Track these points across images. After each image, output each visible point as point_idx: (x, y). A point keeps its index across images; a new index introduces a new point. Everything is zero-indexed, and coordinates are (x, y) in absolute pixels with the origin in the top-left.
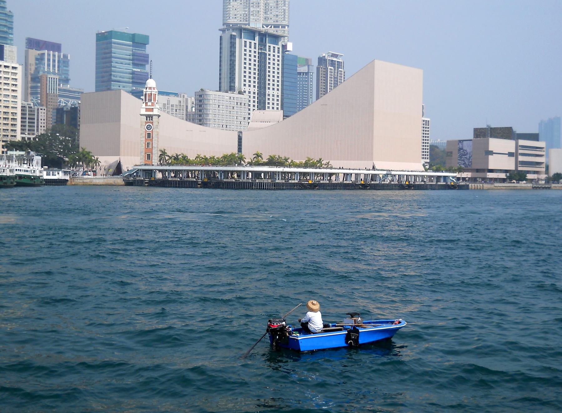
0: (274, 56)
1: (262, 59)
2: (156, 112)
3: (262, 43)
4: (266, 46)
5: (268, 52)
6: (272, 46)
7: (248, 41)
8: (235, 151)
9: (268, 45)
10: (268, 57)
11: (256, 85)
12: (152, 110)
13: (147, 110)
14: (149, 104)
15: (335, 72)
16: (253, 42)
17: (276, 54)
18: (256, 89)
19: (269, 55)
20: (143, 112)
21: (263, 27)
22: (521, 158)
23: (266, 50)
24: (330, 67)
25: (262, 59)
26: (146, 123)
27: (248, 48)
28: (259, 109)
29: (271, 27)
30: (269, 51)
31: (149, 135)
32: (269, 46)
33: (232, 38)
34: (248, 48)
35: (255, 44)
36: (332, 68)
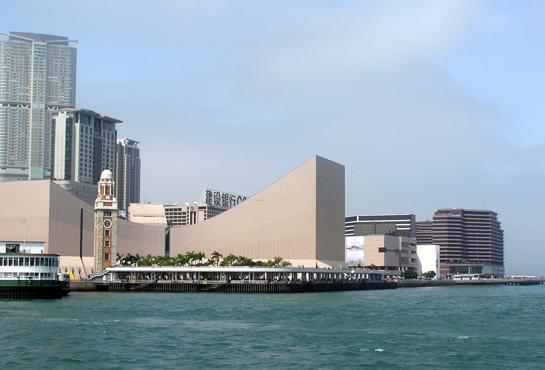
0: (108, 142)
4: (100, 131)
6: (107, 132)
7: (85, 126)
9: (103, 131)
10: (103, 144)
11: (92, 174)
12: (110, 204)
15: (131, 160)
16: (89, 127)
17: (110, 141)
19: (104, 141)
20: (100, 206)
21: (46, 108)
23: (100, 136)
26: (104, 218)
29: (56, 109)
30: (104, 137)
31: (107, 232)
32: (104, 132)
35: (91, 129)
36: (129, 156)
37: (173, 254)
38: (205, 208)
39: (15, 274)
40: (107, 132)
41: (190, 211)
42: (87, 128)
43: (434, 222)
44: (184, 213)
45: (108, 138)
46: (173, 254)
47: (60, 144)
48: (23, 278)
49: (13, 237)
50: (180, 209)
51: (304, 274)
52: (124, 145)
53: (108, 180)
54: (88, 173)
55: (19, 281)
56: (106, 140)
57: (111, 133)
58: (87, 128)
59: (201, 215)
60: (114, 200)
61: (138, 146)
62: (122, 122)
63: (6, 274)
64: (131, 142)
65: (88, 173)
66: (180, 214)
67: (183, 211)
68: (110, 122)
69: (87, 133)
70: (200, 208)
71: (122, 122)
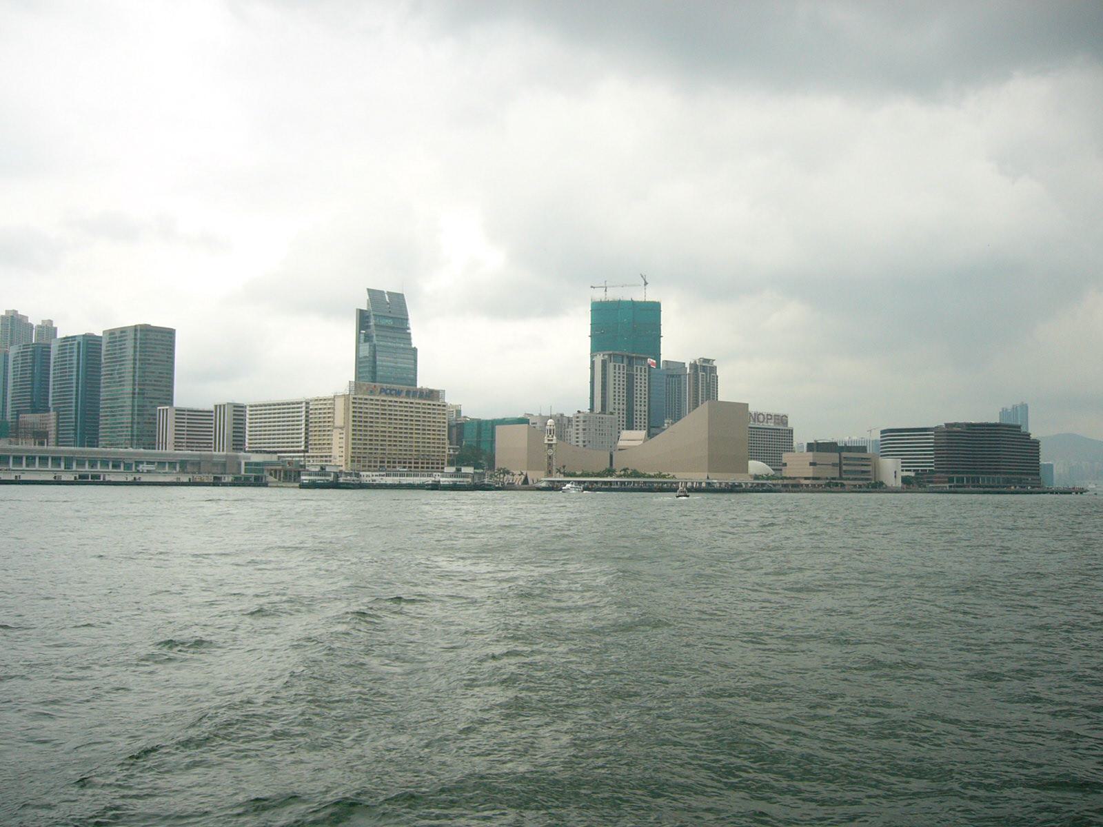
1: (630, 379)
2: (554, 442)
3: (630, 364)
5: (635, 373)
8: (608, 466)
13: (549, 440)
16: (622, 365)
20: (546, 442)
22: (844, 468)
25: (630, 379)
27: (617, 371)
28: (628, 429)
34: (617, 371)
51: (693, 483)
60: (555, 437)
61: (715, 363)
69: (619, 369)
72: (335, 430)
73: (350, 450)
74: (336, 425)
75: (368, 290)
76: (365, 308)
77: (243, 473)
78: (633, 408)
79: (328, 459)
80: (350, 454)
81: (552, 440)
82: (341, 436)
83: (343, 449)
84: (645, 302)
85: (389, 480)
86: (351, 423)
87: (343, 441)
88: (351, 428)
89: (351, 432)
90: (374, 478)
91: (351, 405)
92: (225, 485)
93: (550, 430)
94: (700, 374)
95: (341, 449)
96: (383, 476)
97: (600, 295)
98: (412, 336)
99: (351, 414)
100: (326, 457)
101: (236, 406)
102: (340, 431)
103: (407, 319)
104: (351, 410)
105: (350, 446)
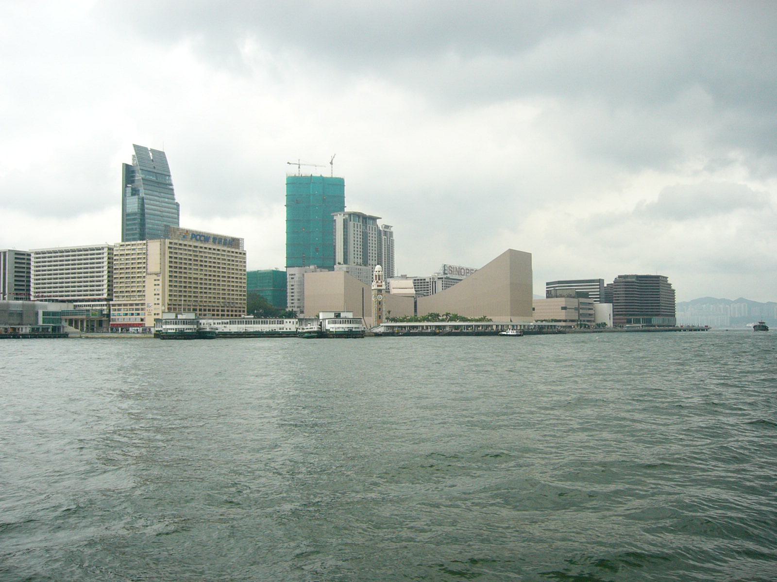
1: (365, 236)
11: (361, 257)
13: (378, 286)
14: (380, 282)
16: (359, 224)
17: (374, 232)
18: (361, 260)
22: (581, 311)
24: (383, 237)
25: (365, 236)
33: (345, 221)
34: (356, 229)
37: (419, 315)
38: (442, 278)
39: (343, 328)
40: (371, 226)
41: (431, 280)
42: (357, 225)
43: (615, 285)
44: (428, 282)
45: (372, 231)
46: (419, 315)
47: (339, 237)
48: (347, 330)
49: (338, 310)
50: (425, 280)
52: (381, 229)
53: (379, 271)
54: (359, 256)
55: (345, 331)
56: (371, 232)
57: (374, 227)
58: (357, 225)
59: (439, 284)
61: (392, 229)
62: (381, 218)
63: (338, 328)
64: (387, 227)
65: (359, 256)
66: (424, 283)
67: (426, 281)
68: (374, 219)
70: (439, 278)
71: (381, 218)
72: (148, 277)
73: (167, 298)
74: (149, 271)
75: (135, 146)
76: (130, 163)
77: (40, 323)
78: (367, 261)
79: (140, 307)
80: (167, 301)
81: (381, 286)
82: (157, 282)
83: (160, 297)
84: (332, 178)
85: (234, 328)
86: (167, 269)
87: (160, 287)
88: (167, 274)
89: (167, 279)
90: (216, 326)
91: (167, 251)
92: (25, 336)
93: (379, 276)
94: (383, 237)
95: (157, 297)
96: (227, 323)
97: (294, 171)
98: (175, 192)
99: (167, 259)
100: (137, 305)
101: (18, 253)
102: (156, 277)
103: (169, 176)
104: (167, 255)
105: (167, 293)
